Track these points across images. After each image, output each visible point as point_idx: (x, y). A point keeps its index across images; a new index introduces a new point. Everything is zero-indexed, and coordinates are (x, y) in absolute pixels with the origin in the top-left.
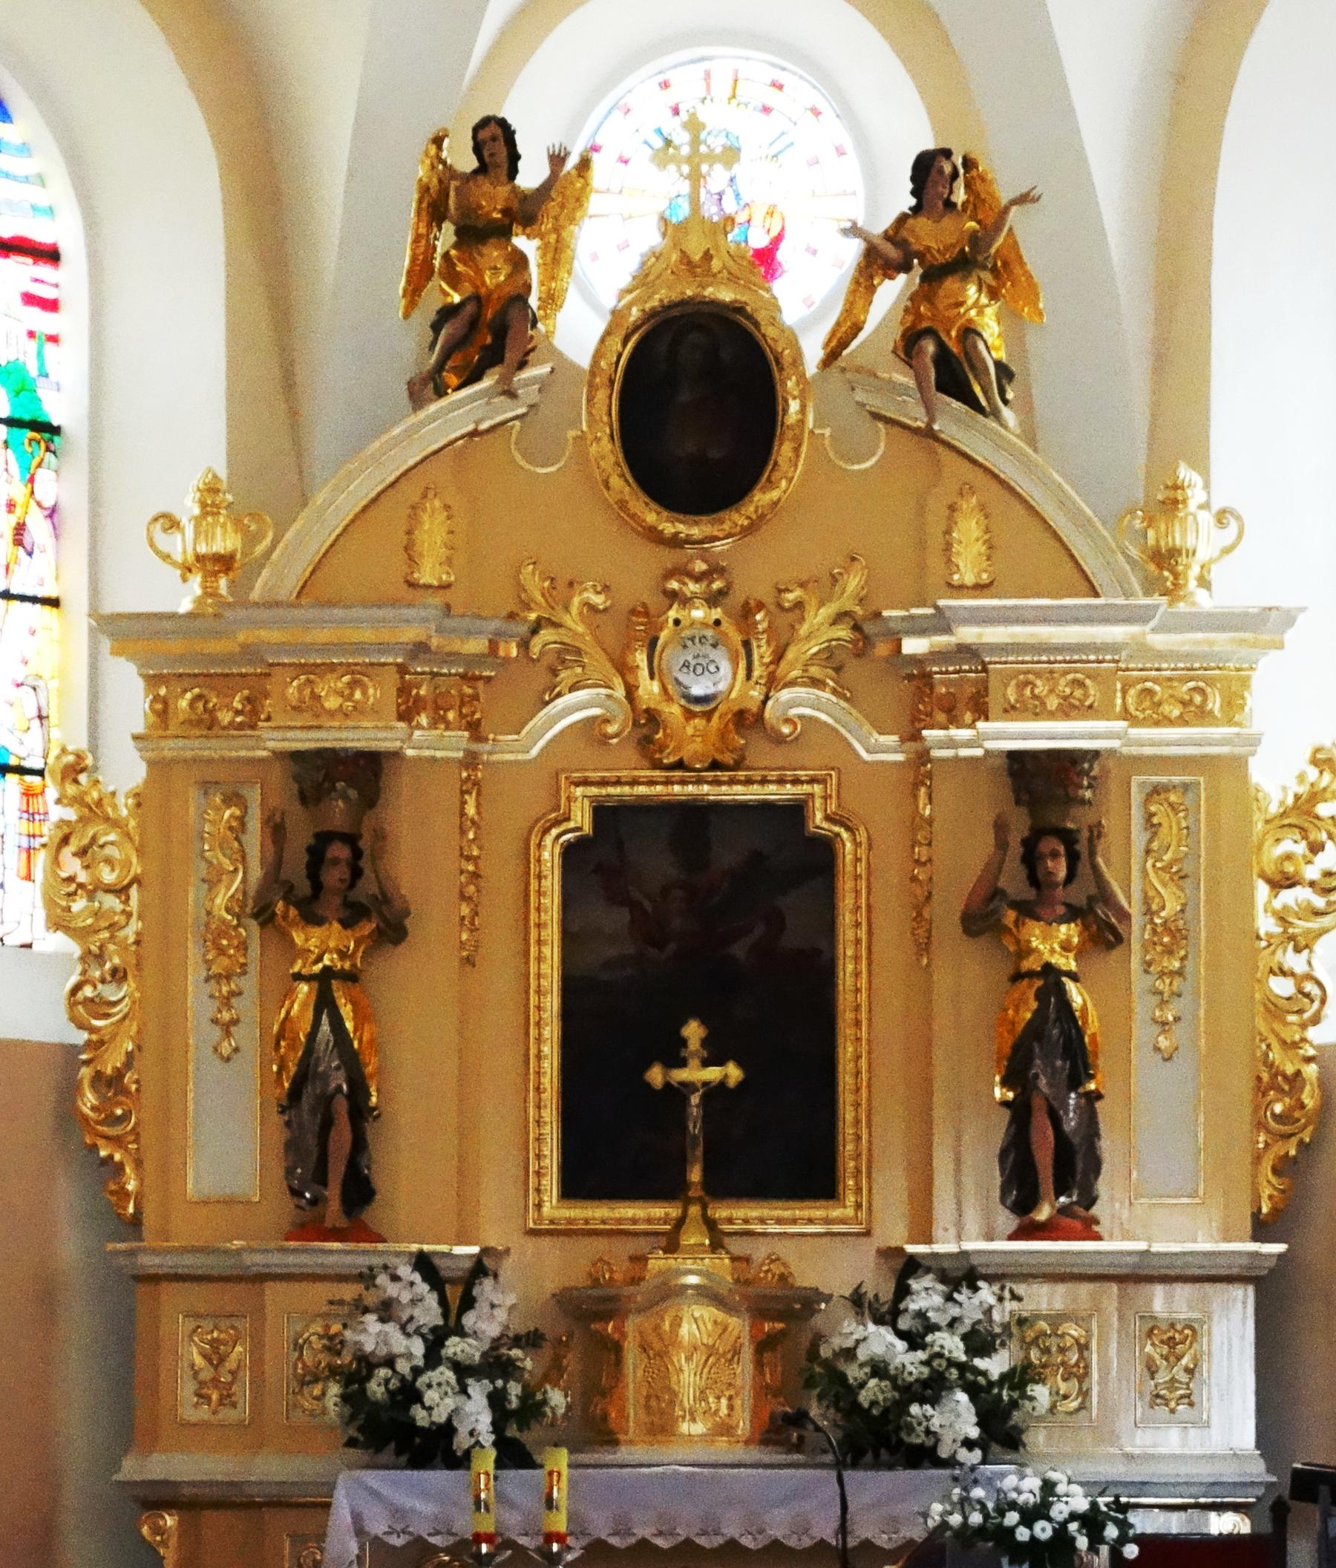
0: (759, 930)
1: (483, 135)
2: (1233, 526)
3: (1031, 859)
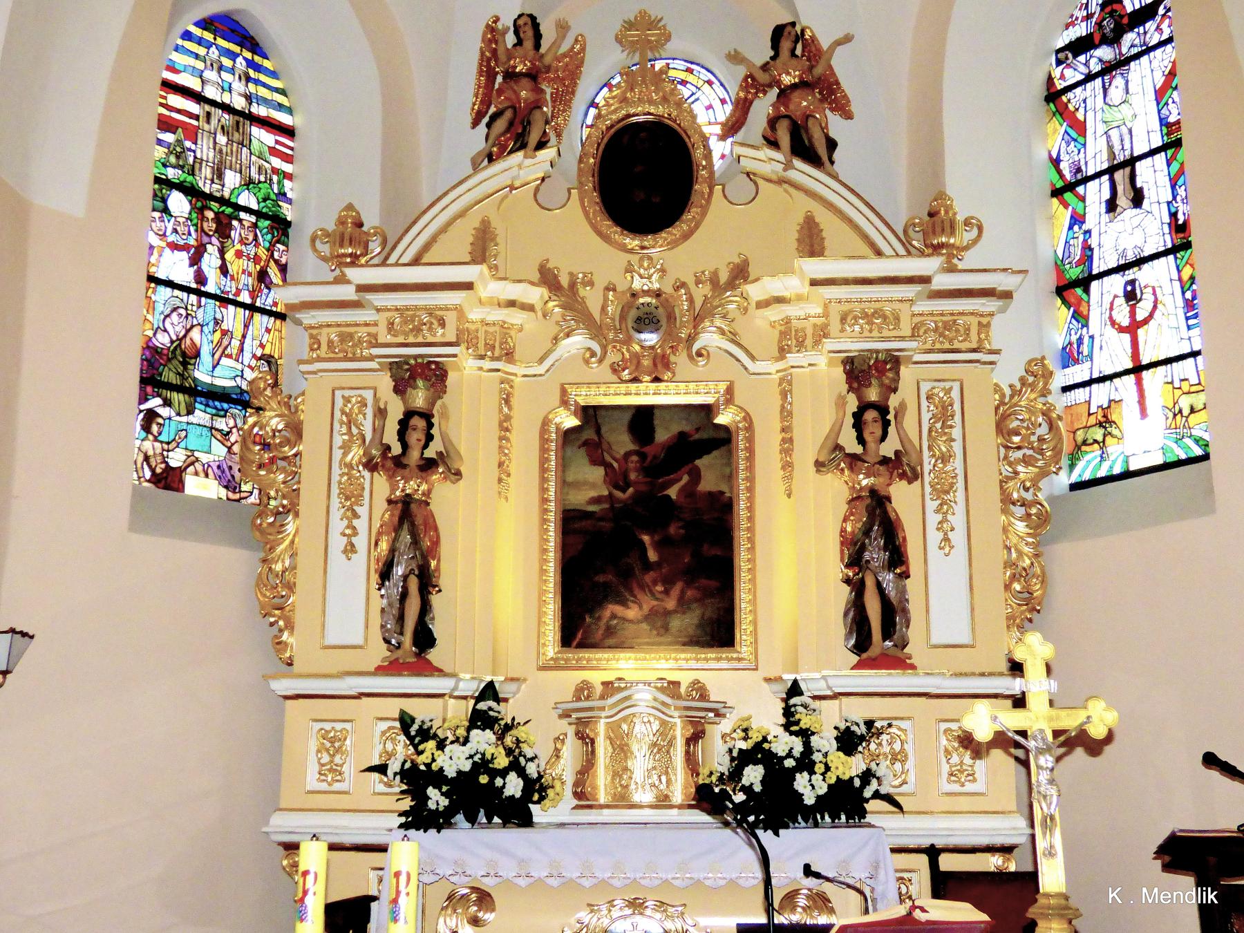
0: (686, 478)
1: (520, 22)
2: (975, 231)
3: (858, 424)
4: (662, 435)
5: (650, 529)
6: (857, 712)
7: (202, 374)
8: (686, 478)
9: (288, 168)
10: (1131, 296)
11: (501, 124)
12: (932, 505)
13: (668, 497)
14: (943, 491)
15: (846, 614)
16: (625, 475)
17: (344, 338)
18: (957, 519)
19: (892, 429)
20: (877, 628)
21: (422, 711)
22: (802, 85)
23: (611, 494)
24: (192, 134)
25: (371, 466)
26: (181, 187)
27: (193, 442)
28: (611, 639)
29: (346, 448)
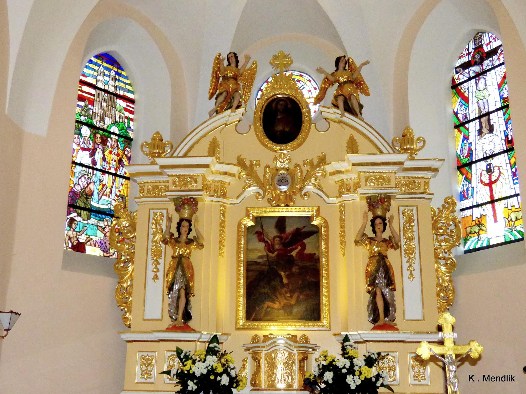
0: (299, 248)
1: (230, 56)
2: (422, 142)
3: (373, 225)
4: (290, 229)
5: (284, 268)
6: (373, 349)
7: (94, 203)
8: (299, 248)
9: (131, 116)
10: (489, 170)
11: (221, 98)
12: (405, 260)
13: (292, 256)
14: (410, 253)
15: (368, 306)
16: (273, 245)
17: (154, 188)
18: (416, 265)
19: (387, 227)
20: (382, 313)
21: (186, 348)
22: (349, 82)
23: (267, 255)
24: (92, 102)
25: (165, 242)
26: (87, 124)
27: (89, 232)
28: (268, 317)
29: (155, 234)
